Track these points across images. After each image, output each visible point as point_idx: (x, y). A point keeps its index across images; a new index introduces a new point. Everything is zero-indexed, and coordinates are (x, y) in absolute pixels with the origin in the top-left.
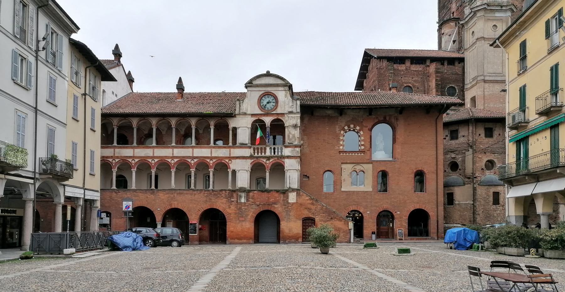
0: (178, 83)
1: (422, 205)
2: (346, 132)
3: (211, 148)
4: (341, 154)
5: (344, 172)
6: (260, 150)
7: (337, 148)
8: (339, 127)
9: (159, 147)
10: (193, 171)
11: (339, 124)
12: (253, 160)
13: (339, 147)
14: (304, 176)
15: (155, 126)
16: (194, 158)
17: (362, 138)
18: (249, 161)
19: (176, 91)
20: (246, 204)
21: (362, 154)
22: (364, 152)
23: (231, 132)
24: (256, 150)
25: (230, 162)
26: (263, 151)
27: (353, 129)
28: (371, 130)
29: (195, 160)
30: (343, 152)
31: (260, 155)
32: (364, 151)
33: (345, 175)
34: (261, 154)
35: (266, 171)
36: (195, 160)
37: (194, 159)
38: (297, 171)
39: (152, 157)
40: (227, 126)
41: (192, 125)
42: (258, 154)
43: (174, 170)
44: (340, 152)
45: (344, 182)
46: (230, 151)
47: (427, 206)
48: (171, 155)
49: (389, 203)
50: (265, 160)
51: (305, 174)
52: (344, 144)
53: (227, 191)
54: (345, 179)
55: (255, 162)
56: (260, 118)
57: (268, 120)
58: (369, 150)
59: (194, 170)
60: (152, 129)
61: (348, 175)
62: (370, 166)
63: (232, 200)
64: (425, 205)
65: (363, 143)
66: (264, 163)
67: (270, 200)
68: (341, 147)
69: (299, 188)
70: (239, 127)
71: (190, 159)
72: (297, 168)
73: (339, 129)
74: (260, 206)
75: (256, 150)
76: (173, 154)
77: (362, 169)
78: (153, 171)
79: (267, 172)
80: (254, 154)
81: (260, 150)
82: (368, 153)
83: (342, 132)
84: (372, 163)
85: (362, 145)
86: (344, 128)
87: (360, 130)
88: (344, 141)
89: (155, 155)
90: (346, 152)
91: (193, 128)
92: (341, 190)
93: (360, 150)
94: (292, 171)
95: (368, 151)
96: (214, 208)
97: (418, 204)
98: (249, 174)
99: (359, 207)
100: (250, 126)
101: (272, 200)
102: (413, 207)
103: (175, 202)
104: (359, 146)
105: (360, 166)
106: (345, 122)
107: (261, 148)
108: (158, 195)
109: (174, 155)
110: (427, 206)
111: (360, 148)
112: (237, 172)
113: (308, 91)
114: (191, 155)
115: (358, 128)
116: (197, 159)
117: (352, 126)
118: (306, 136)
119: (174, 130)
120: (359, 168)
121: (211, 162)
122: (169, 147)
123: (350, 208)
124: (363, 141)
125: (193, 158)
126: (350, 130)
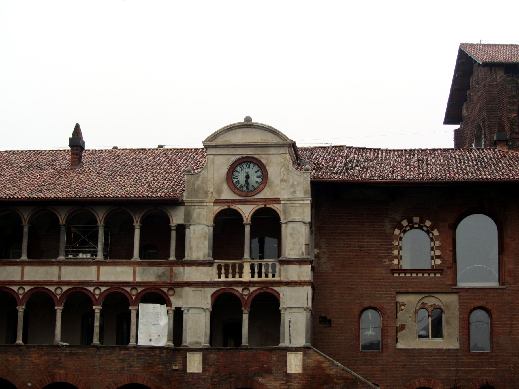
0: (73, 135)
2: (405, 232)
3: (135, 266)
4: (396, 275)
5: (402, 310)
6: (232, 269)
7: (387, 263)
8: (390, 221)
9: (32, 262)
10: (97, 309)
12: (215, 289)
13: (391, 261)
14: (321, 319)
15: (27, 222)
16: (101, 284)
17: (438, 243)
18: (210, 291)
19: (69, 148)
20: (202, 377)
21: (438, 275)
22: (441, 271)
23: (173, 234)
24: (223, 268)
25: (171, 293)
26: (237, 270)
27: (419, 225)
28: (454, 227)
29: (103, 289)
30: (398, 271)
31: (230, 279)
32: (440, 268)
33: (403, 317)
34: (234, 277)
35: (242, 311)
36: (103, 289)
37: (101, 286)
38: (304, 309)
39: (18, 282)
40: (167, 220)
41: (99, 222)
42: (227, 277)
43: (60, 308)
44: (393, 271)
45: (402, 330)
46: (172, 270)
48: (56, 279)
50: (242, 288)
51: (323, 315)
52: (401, 254)
53: (164, 351)
55: (221, 292)
56: (231, 207)
58: (451, 267)
59: (100, 307)
60: (22, 228)
61: (410, 317)
62: (454, 298)
63: (174, 367)
65: (438, 253)
66: (238, 295)
67: (250, 369)
68: (396, 262)
69: (309, 344)
71: (93, 286)
72: (305, 305)
75: (223, 268)
76: (60, 277)
77: (438, 303)
78: (21, 310)
79: (244, 312)
80: (220, 277)
81: (230, 268)
82: (449, 273)
83: (397, 232)
84: (457, 293)
85: (438, 257)
86: (400, 223)
87: (432, 228)
88: (401, 249)
89: (26, 278)
90: (405, 271)
91: (101, 224)
92: (396, 346)
93: (433, 266)
94: (294, 310)
95: (449, 269)
96: (138, 382)
98: (209, 316)
99: (433, 381)
100: (212, 223)
101: (254, 368)
103: (62, 371)
104: (432, 258)
105: (435, 298)
107: (234, 266)
108: (30, 357)
109: (63, 279)
111: (433, 264)
112: (185, 312)
113: (333, 145)
114: (95, 279)
115: (428, 223)
116: (107, 286)
117: (416, 219)
118: (324, 240)
119: (63, 228)
120: (433, 304)
121: (134, 292)
122: (51, 264)
123: (416, 385)
124: (438, 250)
125: (98, 284)
126: (412, 228)
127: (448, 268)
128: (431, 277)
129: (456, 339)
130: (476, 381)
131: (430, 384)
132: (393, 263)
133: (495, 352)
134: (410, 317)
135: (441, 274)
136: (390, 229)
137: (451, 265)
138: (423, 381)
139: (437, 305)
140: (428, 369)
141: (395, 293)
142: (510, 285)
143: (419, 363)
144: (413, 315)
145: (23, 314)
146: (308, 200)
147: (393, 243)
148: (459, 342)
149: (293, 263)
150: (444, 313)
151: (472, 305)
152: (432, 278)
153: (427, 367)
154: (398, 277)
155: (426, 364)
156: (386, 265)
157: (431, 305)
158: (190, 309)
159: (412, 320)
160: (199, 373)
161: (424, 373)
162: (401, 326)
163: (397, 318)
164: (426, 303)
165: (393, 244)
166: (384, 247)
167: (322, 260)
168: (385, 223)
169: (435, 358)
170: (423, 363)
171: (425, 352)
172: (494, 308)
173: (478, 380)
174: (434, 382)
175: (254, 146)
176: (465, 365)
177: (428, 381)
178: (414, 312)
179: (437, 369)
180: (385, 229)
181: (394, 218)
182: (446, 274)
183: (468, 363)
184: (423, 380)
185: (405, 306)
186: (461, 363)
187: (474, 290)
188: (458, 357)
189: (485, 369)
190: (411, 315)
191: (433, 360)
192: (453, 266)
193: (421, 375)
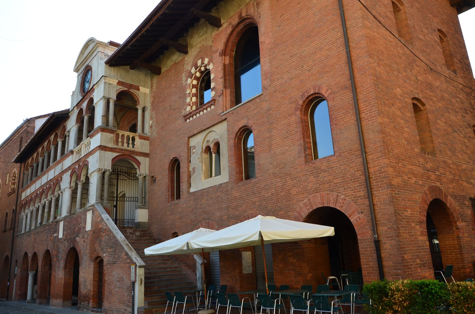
1: (328, 194)
4: (188, 121)
13: (185, 109)
21: (213, 107)
44: (186, 117)
47: (342, 196)
49: (257, 203)
57: (84, 105)
64: (335, 194)
70: (70, 129)
74: (69, 241)
79: (79, 184)
82: (220, 101)
83: (189, 80)
86: (190, 72)
97: (318, 194)
99: (211, 224)
102: (305, 205)
106: (192, 61)
110: (342, 196)
130: (243, 218)
131: (209, 226)
134: (198, 158)
135: (214, 105)
140: (207, 210)
143: (201, 205)
145: (35, 211)
146: (102, 80)
147: (187, 92)
149: (94, 135)
154: (189, 122)
158: (66, 189)
159: (199, 161)
160: (61, 238)
161: (205, 215)
163: (190, 163)
167: (154, 128)
172: (254, 123)
173: (244, 216)
174: (212, 223)
175: (88, 56)
177: (207, 224)
183: (236, 196)
184: (204, 223)
186: (230, 198)
189: (249, 201)
191: (211, 199)
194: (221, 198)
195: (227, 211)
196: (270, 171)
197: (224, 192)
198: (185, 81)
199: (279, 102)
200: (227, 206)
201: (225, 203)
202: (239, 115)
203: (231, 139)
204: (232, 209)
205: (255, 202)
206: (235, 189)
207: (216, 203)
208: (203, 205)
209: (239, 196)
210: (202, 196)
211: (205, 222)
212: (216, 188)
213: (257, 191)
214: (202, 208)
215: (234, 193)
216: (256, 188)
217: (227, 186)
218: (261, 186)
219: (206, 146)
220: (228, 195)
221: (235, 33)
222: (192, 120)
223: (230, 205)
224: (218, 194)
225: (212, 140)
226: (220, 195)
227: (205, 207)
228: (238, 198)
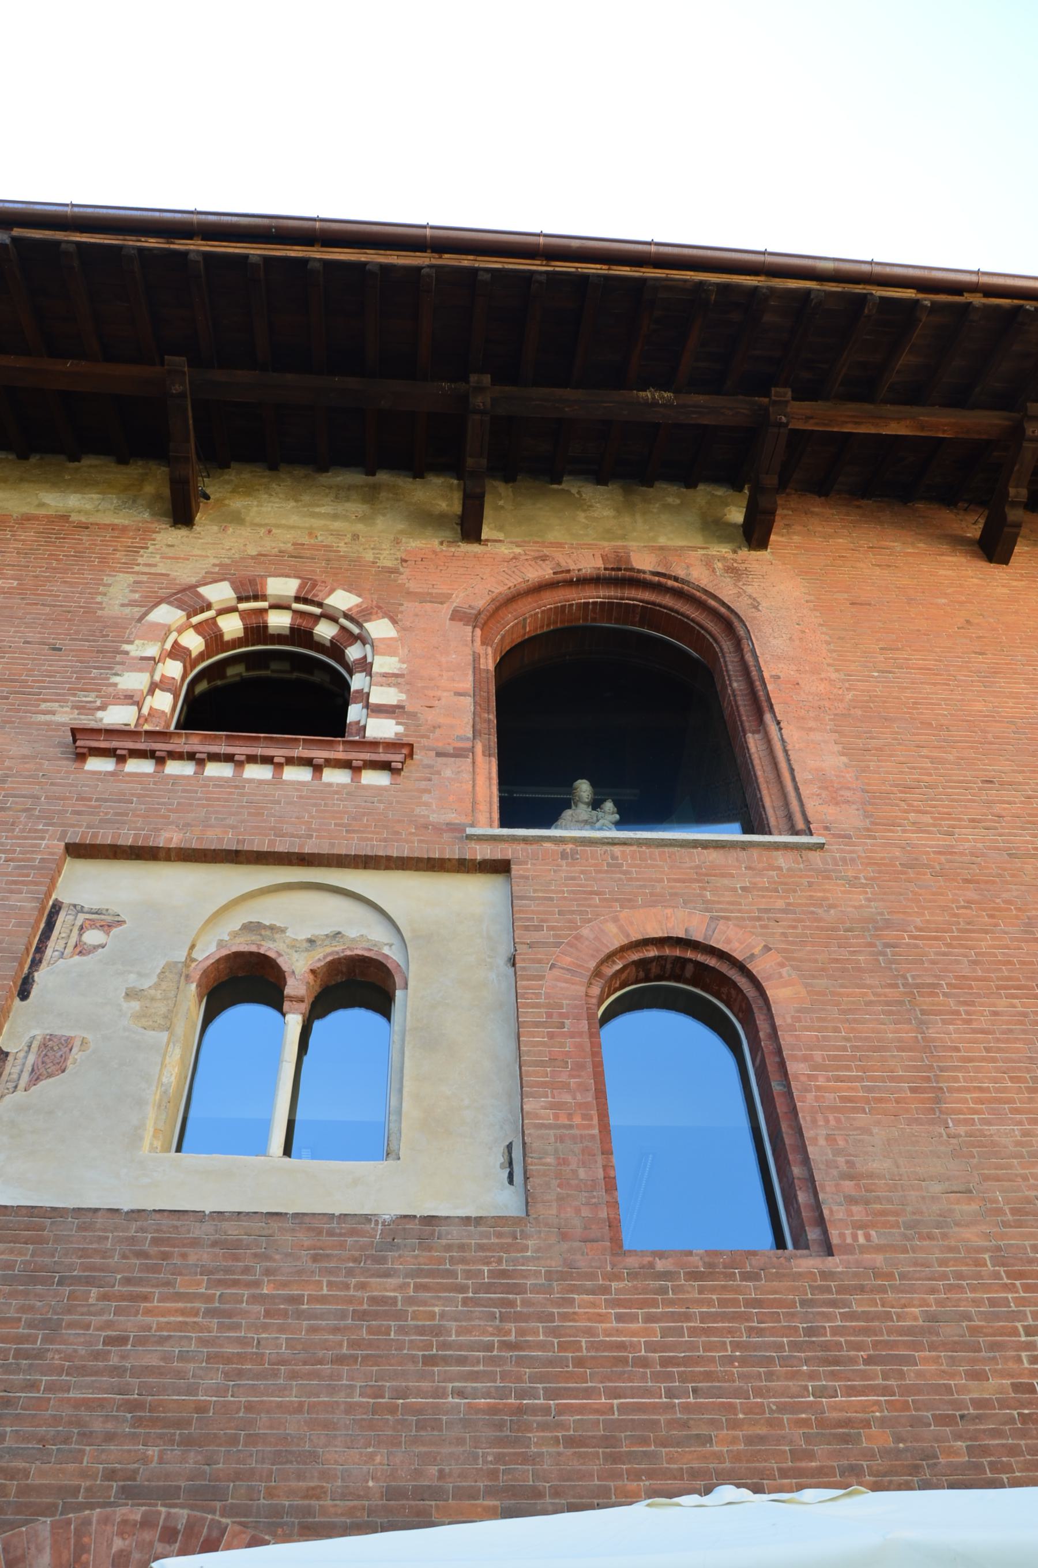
5: (82, 950)
11: (137, 568)
22: (395, 758)
54: (67, 1043)
73: (137, 596)
82: (448, 773)
83: (166, 614)
127: (439, 754)
128: (330, 785)
129: (498, 1158)
132: (101, 720)
133: (848, 1249)
136: (123, 605)
137: (469, 745)
138: (118, 1544)
139: (353, 940)
140: (201, 1408)
141: (63, 844)
142: (849, 837)
143: (122, 1340)
144: (157, 986)
148: (518, 1177)
150: (406, 987)
151: (612, 928)
152: (337, 793)
153: (192, 1390)
155: (183, 1357)
156: (48, 724)
157: (311, 941)
161: (153, 1451)
162: (44, 1045)
163: (24, 994)
164: (272, 928)
165: (127, 653)
166: (69, 661)
168: (109, 585)
169: (297, 1300)
170: (162, 1341)
171: (195, 1243)
172: (767, 949)
176: (580, 1362)
178: (170, 966)
179: (299, 1408)
180: (100, 603)
181: (167, 575)
182: (430, 780)
183: (621, 1346)
184: (125, 1527)
185: (115, 931)
186: (542, 1346)
187: (617, 850)
188: (518, 1289)
189: (782, 1408)
190: (146, 984)
192: (472, 750)
193: (111, 1475)
194: (421, 1331)
195: (499, 1458)
196: (971, 1235)
197: (463, 1289)
198: (123, 605)
199: (955, 915)
200: (493, 1410)
201: (474, 1376)
202: (631, 879)
203: (556, 972)
204: (571, 1442)
205: (848, 1423)
206: (606, 1290)
207: (340, 1360)
208: (140, 1341)
209: (650, 1347)
210: (155, 1269)
211: (147, 1523)
212: (353, 1232)
213: (859, 1347)
214: (117, 1371)
215: (601, 1318)
216: (844, 1317)
217: (506, 1248)
218: (900, 1317)
219: (234, 949)
220: (519, 1317)
221: (551, 600)
222: (147, 775)
223: (546, 1410)
224: (388, 1288)
225: (304, 935)
226: (410, 1301)
227: (180, 1374)
228: (644, 1363)
